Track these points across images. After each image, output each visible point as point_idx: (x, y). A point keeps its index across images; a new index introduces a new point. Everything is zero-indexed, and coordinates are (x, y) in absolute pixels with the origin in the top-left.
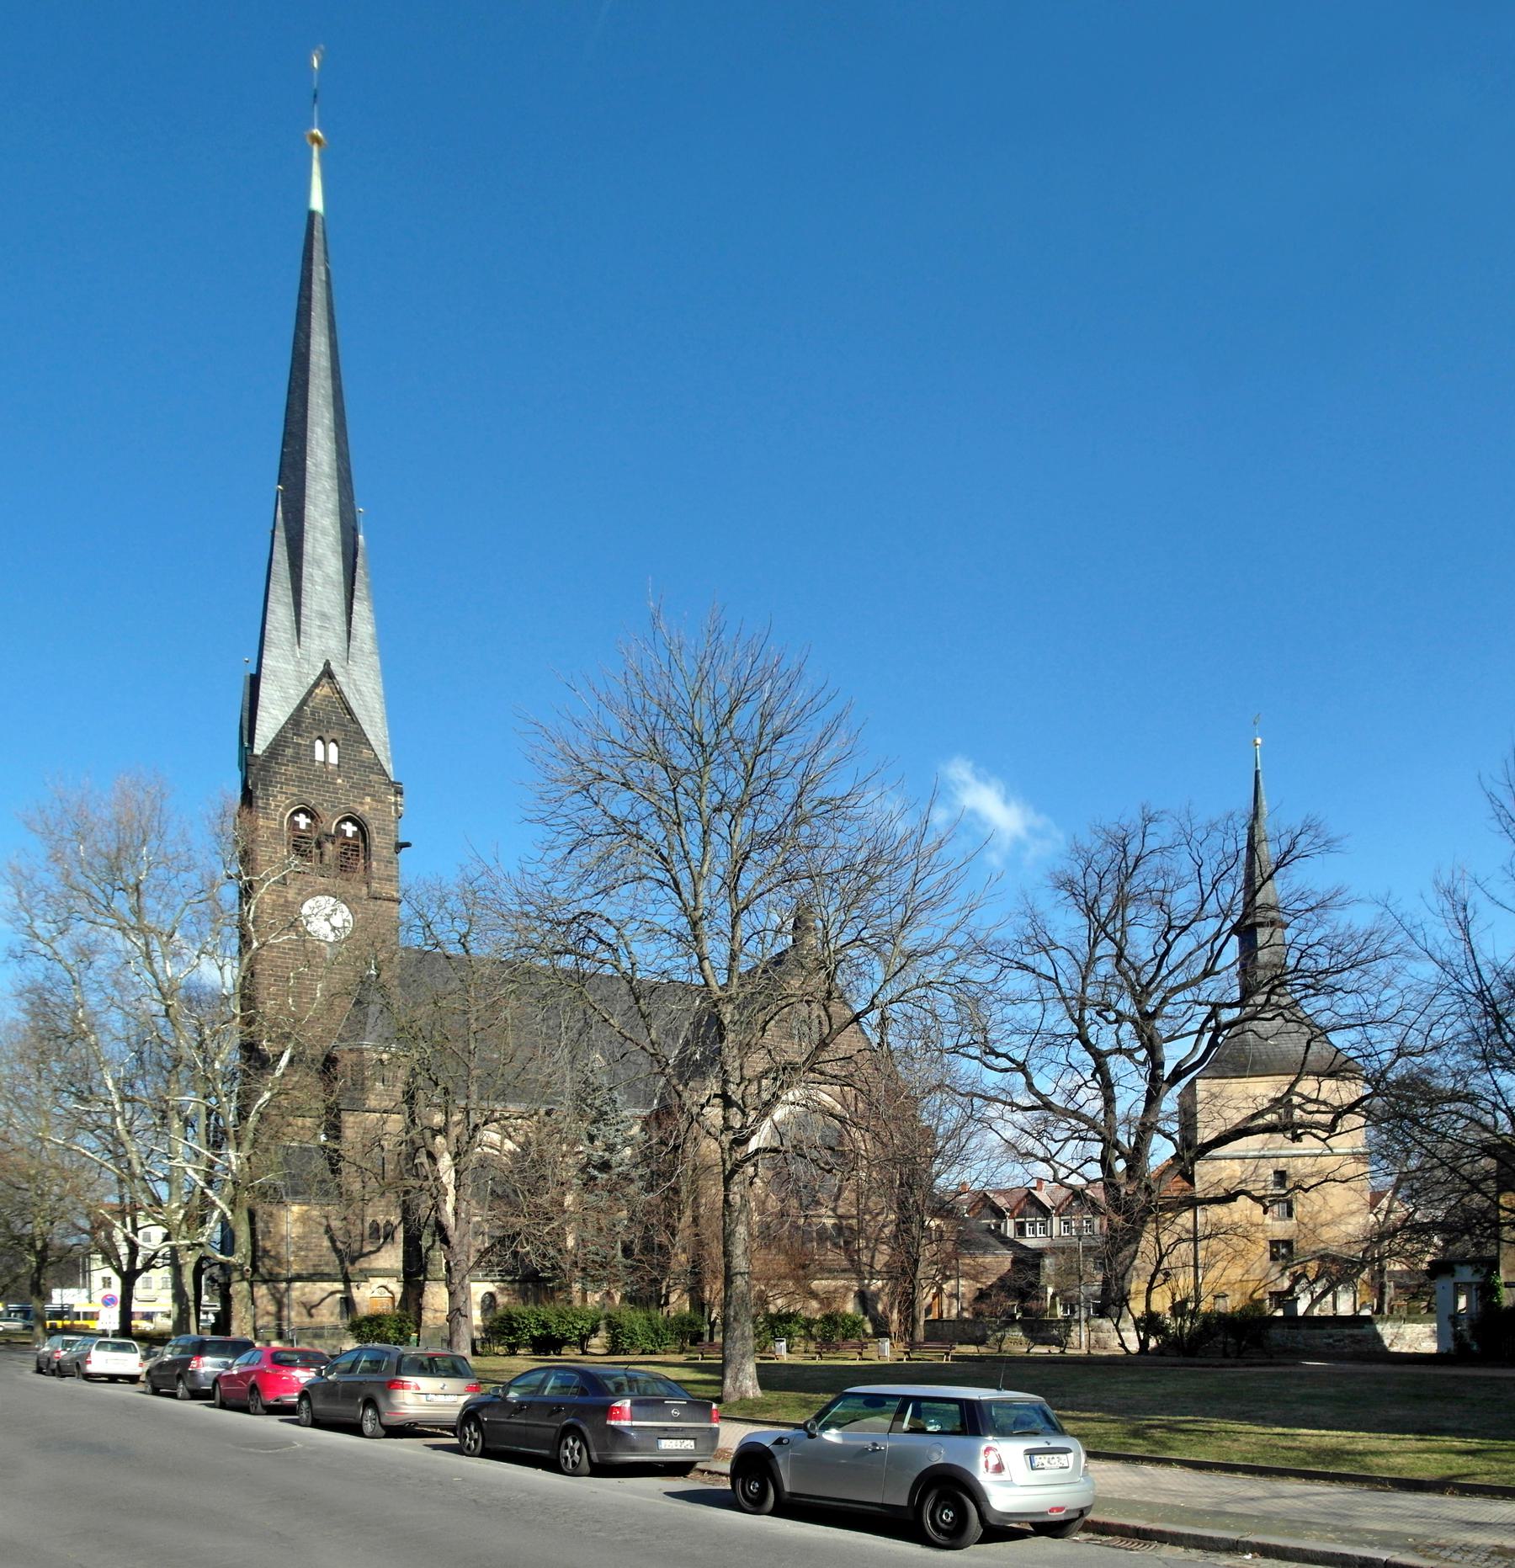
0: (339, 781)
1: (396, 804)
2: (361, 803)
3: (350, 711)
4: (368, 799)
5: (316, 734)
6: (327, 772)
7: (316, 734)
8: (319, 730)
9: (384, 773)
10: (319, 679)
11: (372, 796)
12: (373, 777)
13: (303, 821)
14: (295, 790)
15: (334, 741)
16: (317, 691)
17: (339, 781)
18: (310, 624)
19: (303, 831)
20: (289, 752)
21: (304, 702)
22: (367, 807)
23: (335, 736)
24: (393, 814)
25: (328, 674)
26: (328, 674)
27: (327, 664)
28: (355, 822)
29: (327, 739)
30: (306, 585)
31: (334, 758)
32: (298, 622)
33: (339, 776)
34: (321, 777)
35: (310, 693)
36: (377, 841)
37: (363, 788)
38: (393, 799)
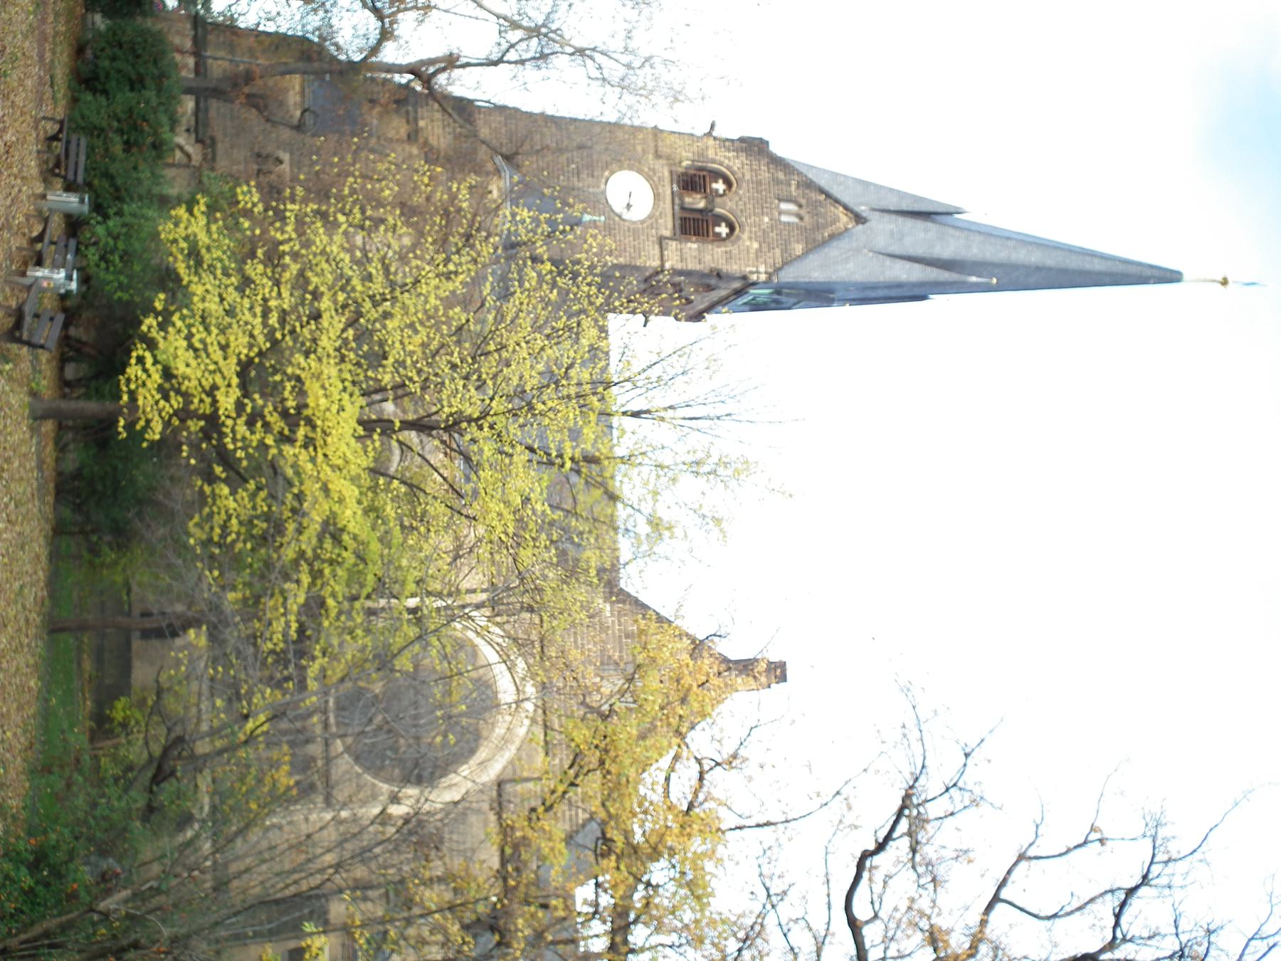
1: (758, 272)
3: (832, 237)
4: (756, 245)
5: (803, 202)
9: (785, 264)
11: (759, 250)
12: (778, 252)
14: (748, 177)
16: (841, 209)
17: (766, 219)
20: (781, 175)
21: (828, 196)
22: (748, 243)
24: (748, 269)
25: (859, 219)
31: (784, 218)
35: (837, 201)
37: (763, 238)
38: (762, 269)
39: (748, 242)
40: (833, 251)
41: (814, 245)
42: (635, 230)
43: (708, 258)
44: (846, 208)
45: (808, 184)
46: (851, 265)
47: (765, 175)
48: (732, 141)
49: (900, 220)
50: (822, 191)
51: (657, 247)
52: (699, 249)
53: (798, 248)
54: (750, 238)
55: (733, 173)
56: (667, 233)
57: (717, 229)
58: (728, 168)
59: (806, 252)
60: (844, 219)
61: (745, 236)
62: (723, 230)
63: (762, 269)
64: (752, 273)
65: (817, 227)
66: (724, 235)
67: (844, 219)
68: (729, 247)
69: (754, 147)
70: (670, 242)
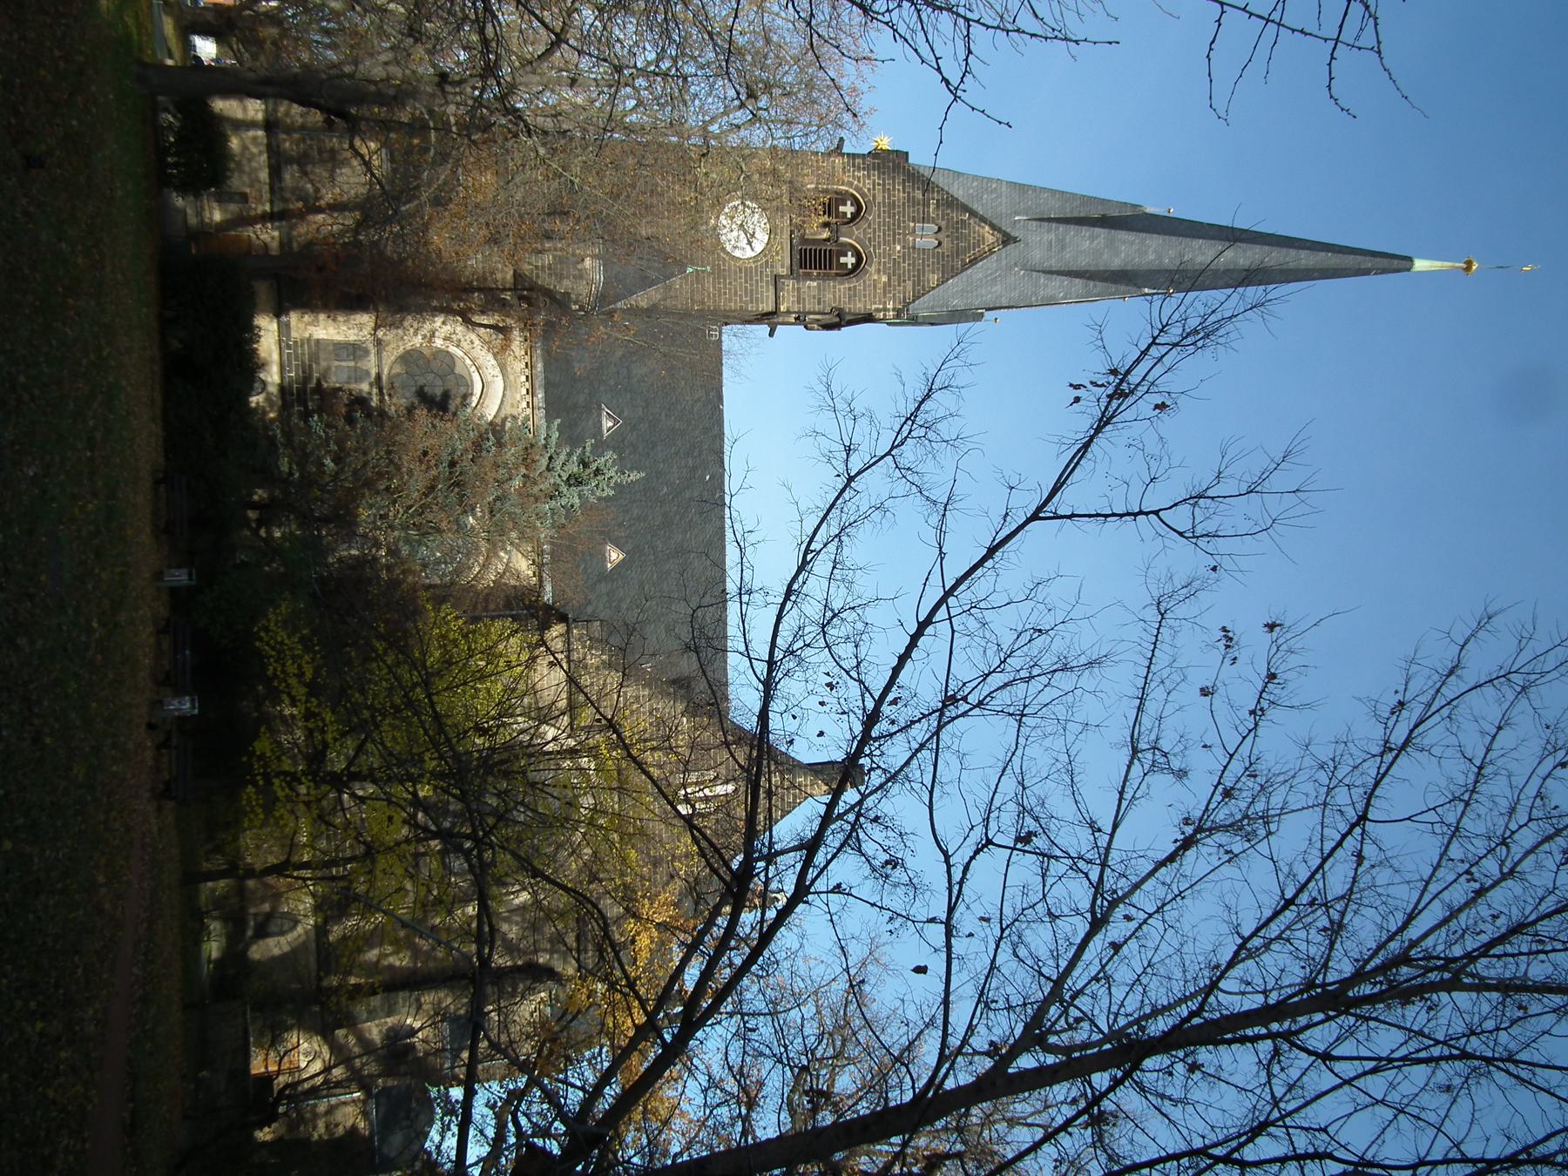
0: (898, 248)
1: (885, 309)
2: (879, 271)
3: (974, 262)
4: (884, 279)
5: (943, 224)
6: (905, 235)
7: (943, 224)
8: (947, 227)
9: (916, 298)
10: (1000, 230)
12: (909, 284)
13: (848, 209)
15: (940, 244)
16: (987, 228)
17: (898, 248)
18: (1051, 234)
19: (837, 209)
21: (973, 214)
23: (945, 244)
24: (874, 307)
25: (1007, 240)
26: (1007, 240)
27: (1015, 240)
28: (857, 266)
29: (941, 236)
30: (1086, 231)
32: (1050, 220)
33: (904, 247)
34: (899, 228)
35: (983, 220)
36: (837, 293)
37: (894, 271)
38: (890, 306)
39: (876, 275)
40: (976, 272)
41: (949, 273)
42: (746, 270)
43: (829, 296)
44: (993, 227)
45: (951, 203)
46: (998, 288)
47: (900, 195)
48: (863, 156)
49: (1062, 228)
50: (965, 208)
51: (772, 288)
52: (819, 285)
53: (934, 278)
54: (879, 271)
55: (863, 195)
56: (784, 271)
57: (843, 260)
58: (858, 189)
59: (943, 281)
60: (990, 237)
61: (873, 269)
62: (849, 260)
63: (890, 306)
64: (878, 310)
65: (958, 253)
66: (850, 266)
67: (990, 239)
68: (854, 283)
69: (891, 163)
70: (786, 282)
